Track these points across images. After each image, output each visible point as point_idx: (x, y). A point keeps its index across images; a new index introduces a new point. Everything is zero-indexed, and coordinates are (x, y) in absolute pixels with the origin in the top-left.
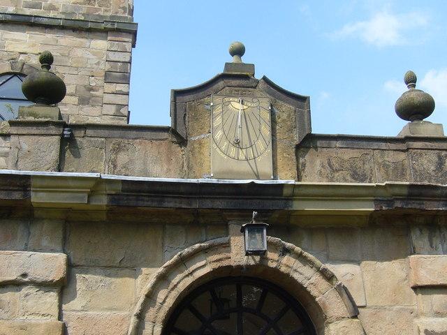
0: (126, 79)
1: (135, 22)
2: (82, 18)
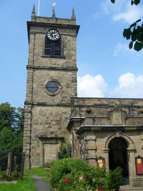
0: (76, 82)
1: (77, 68)
2: (65, 67)
